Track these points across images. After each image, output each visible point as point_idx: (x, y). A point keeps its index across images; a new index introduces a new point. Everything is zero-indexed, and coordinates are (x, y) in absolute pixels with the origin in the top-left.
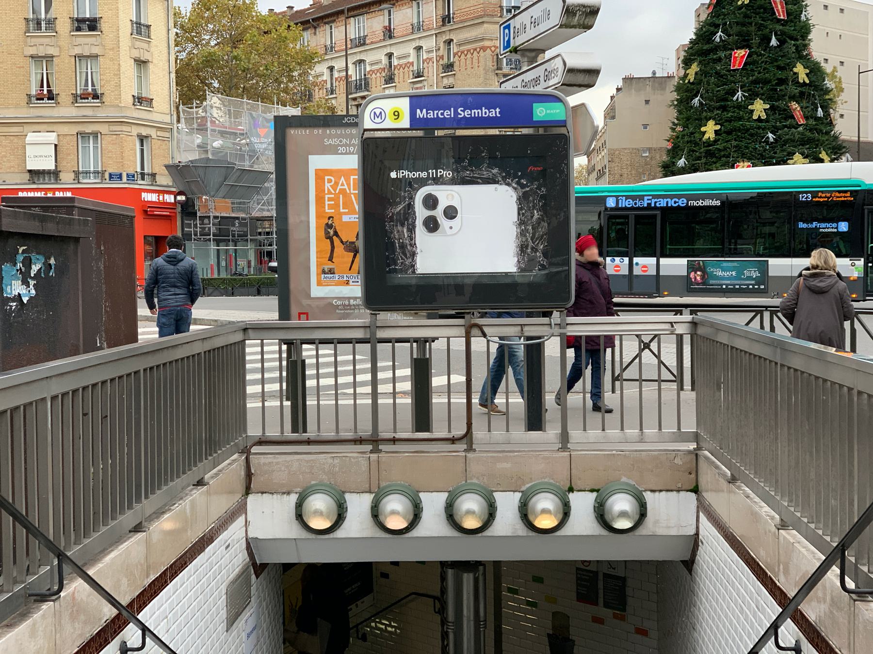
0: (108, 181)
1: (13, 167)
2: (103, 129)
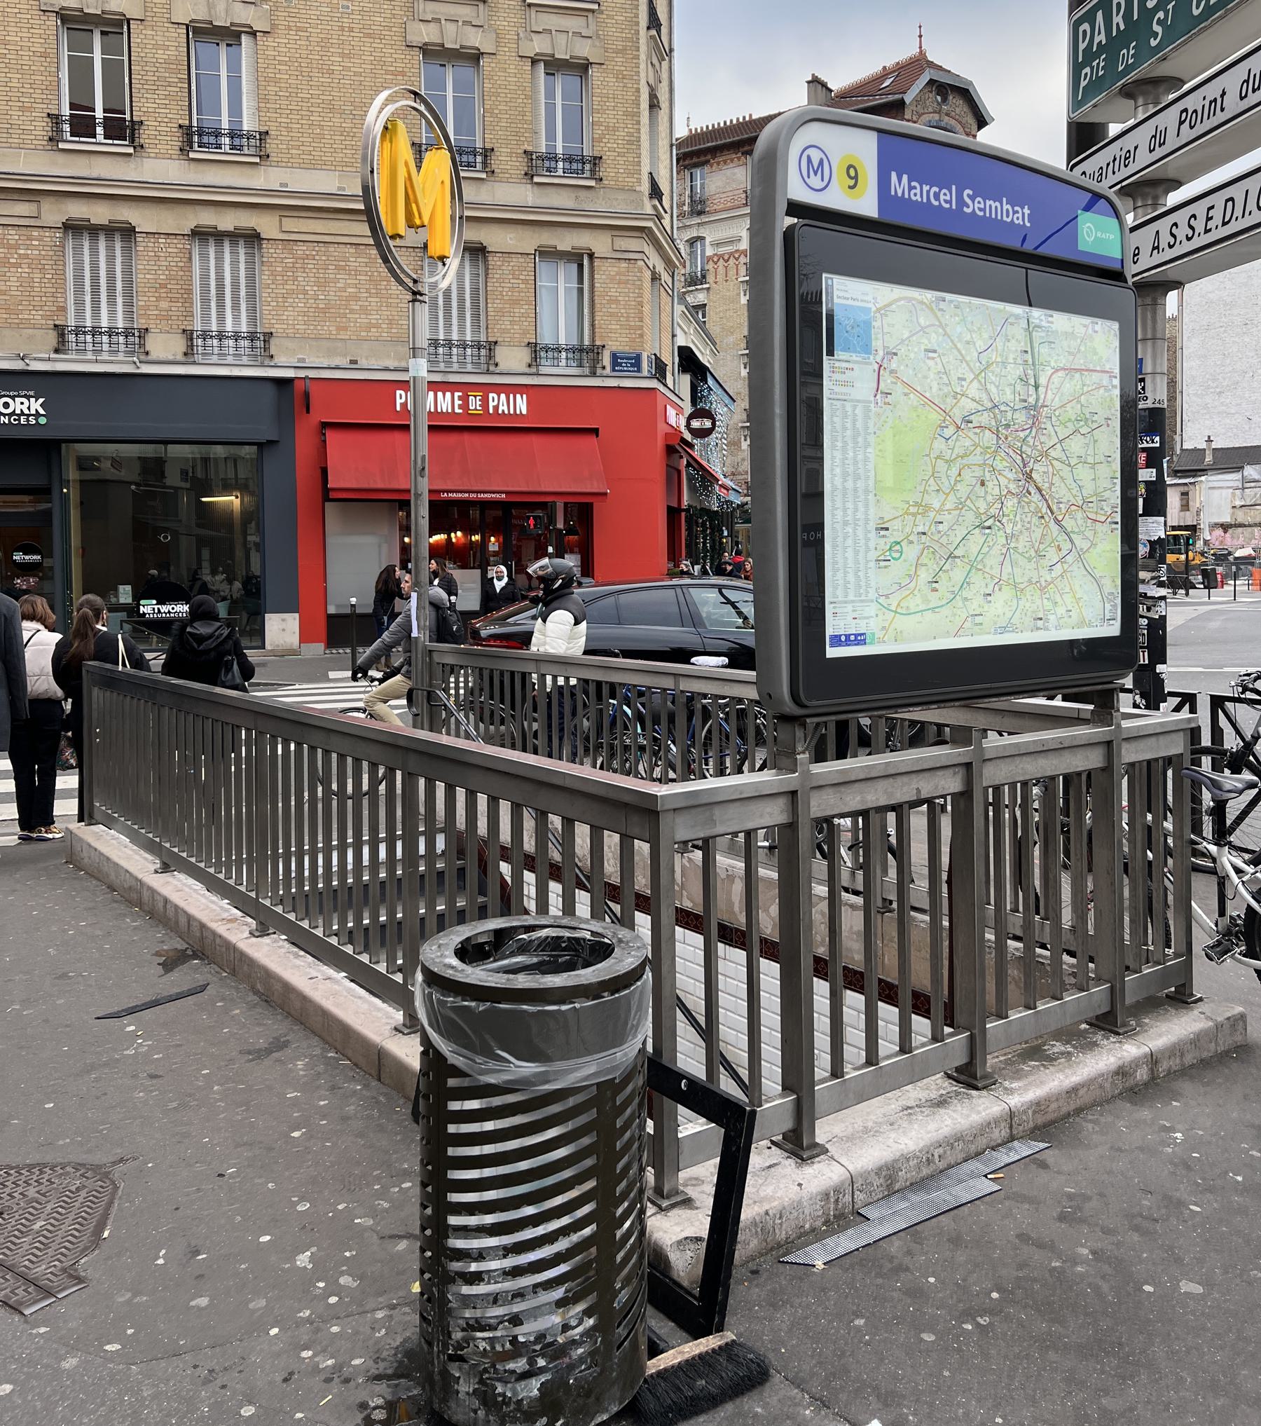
0: (608, 371)
1: (377, 326)
2: (600, 244)
